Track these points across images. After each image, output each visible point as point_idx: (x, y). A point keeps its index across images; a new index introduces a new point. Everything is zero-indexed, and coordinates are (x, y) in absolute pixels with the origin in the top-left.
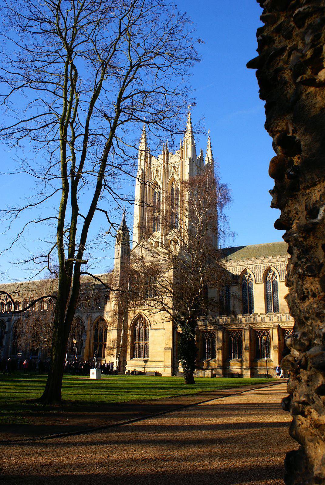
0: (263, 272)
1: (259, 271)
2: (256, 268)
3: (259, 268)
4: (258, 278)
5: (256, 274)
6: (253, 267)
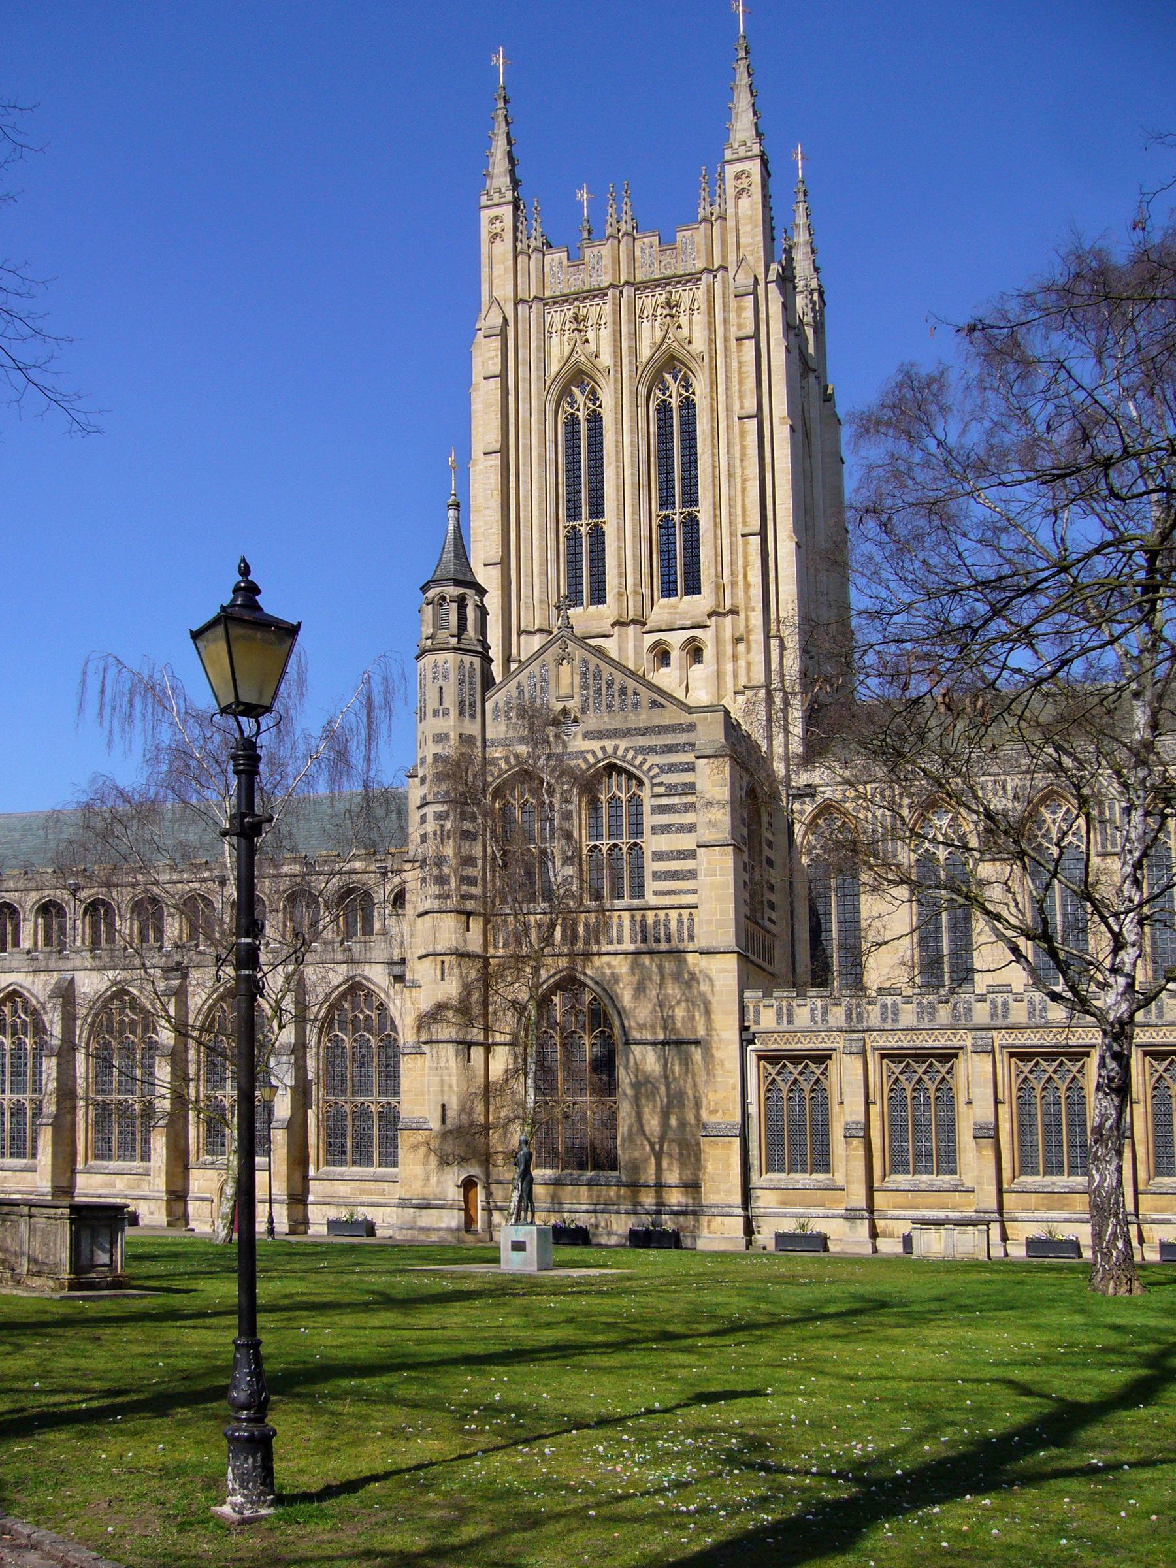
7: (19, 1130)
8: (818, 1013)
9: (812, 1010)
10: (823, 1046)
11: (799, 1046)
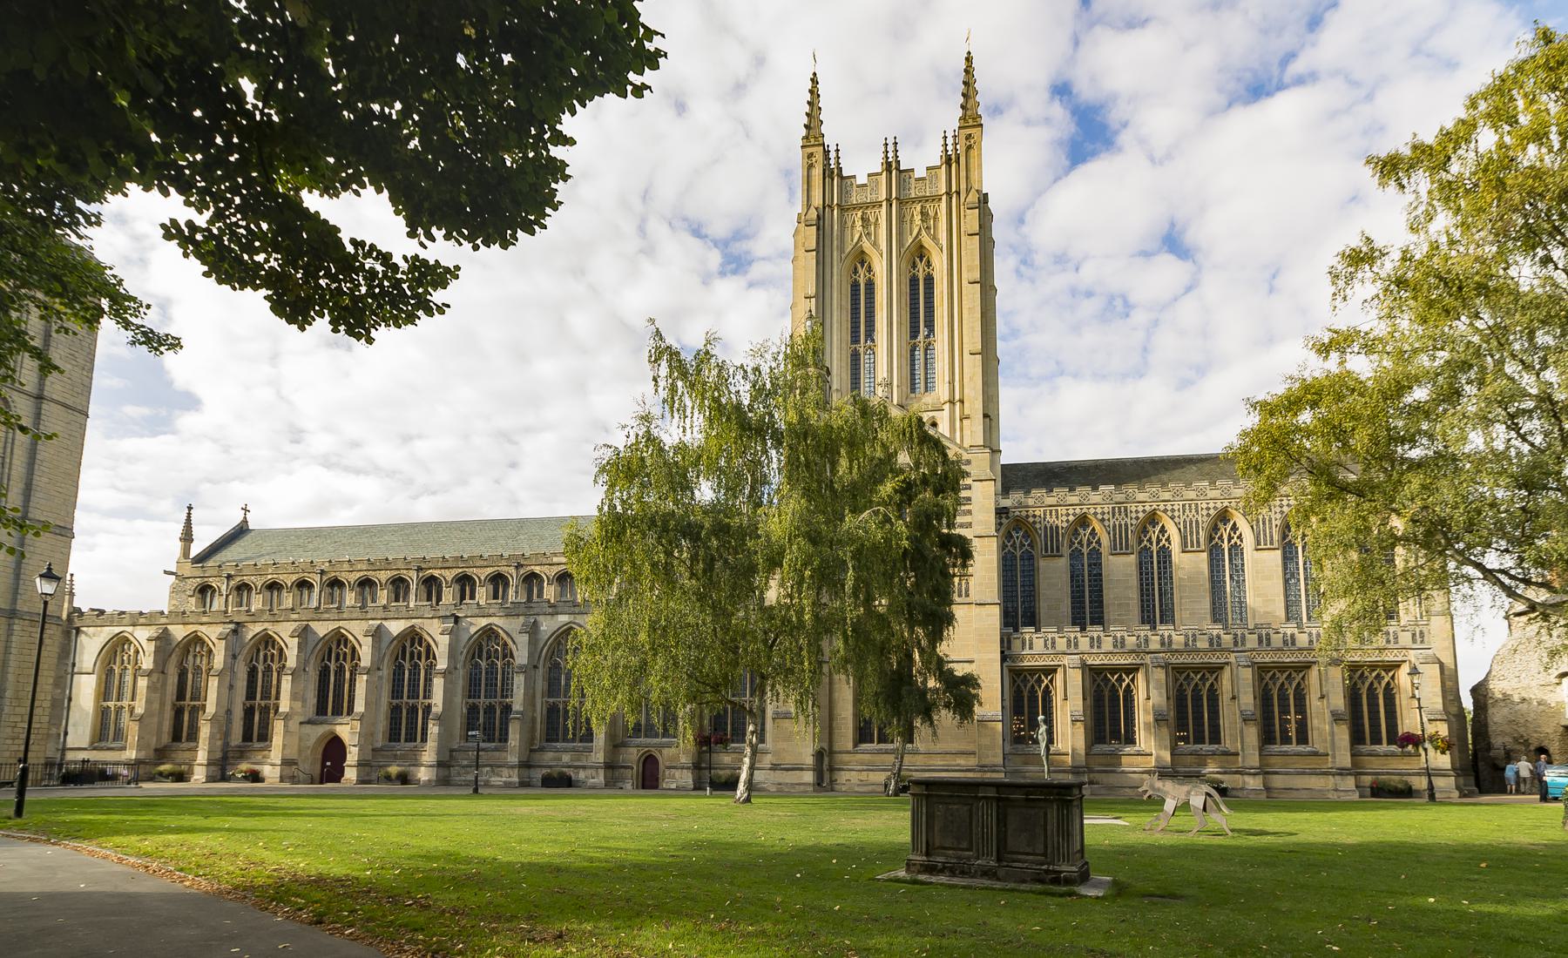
0: (1204, 521)
1: (1194, 520)
2: (1184, 511)
3: (1193, 511)
4: (1191, 536)
5: (1185, 527)
6: (1176, 507)
7: (490, 723)
8: (1049, 642)
9: (1045, 641)
10: (1052, 663)
11: (1037, 663)
